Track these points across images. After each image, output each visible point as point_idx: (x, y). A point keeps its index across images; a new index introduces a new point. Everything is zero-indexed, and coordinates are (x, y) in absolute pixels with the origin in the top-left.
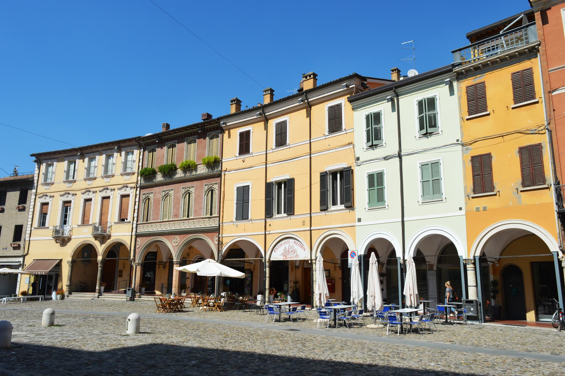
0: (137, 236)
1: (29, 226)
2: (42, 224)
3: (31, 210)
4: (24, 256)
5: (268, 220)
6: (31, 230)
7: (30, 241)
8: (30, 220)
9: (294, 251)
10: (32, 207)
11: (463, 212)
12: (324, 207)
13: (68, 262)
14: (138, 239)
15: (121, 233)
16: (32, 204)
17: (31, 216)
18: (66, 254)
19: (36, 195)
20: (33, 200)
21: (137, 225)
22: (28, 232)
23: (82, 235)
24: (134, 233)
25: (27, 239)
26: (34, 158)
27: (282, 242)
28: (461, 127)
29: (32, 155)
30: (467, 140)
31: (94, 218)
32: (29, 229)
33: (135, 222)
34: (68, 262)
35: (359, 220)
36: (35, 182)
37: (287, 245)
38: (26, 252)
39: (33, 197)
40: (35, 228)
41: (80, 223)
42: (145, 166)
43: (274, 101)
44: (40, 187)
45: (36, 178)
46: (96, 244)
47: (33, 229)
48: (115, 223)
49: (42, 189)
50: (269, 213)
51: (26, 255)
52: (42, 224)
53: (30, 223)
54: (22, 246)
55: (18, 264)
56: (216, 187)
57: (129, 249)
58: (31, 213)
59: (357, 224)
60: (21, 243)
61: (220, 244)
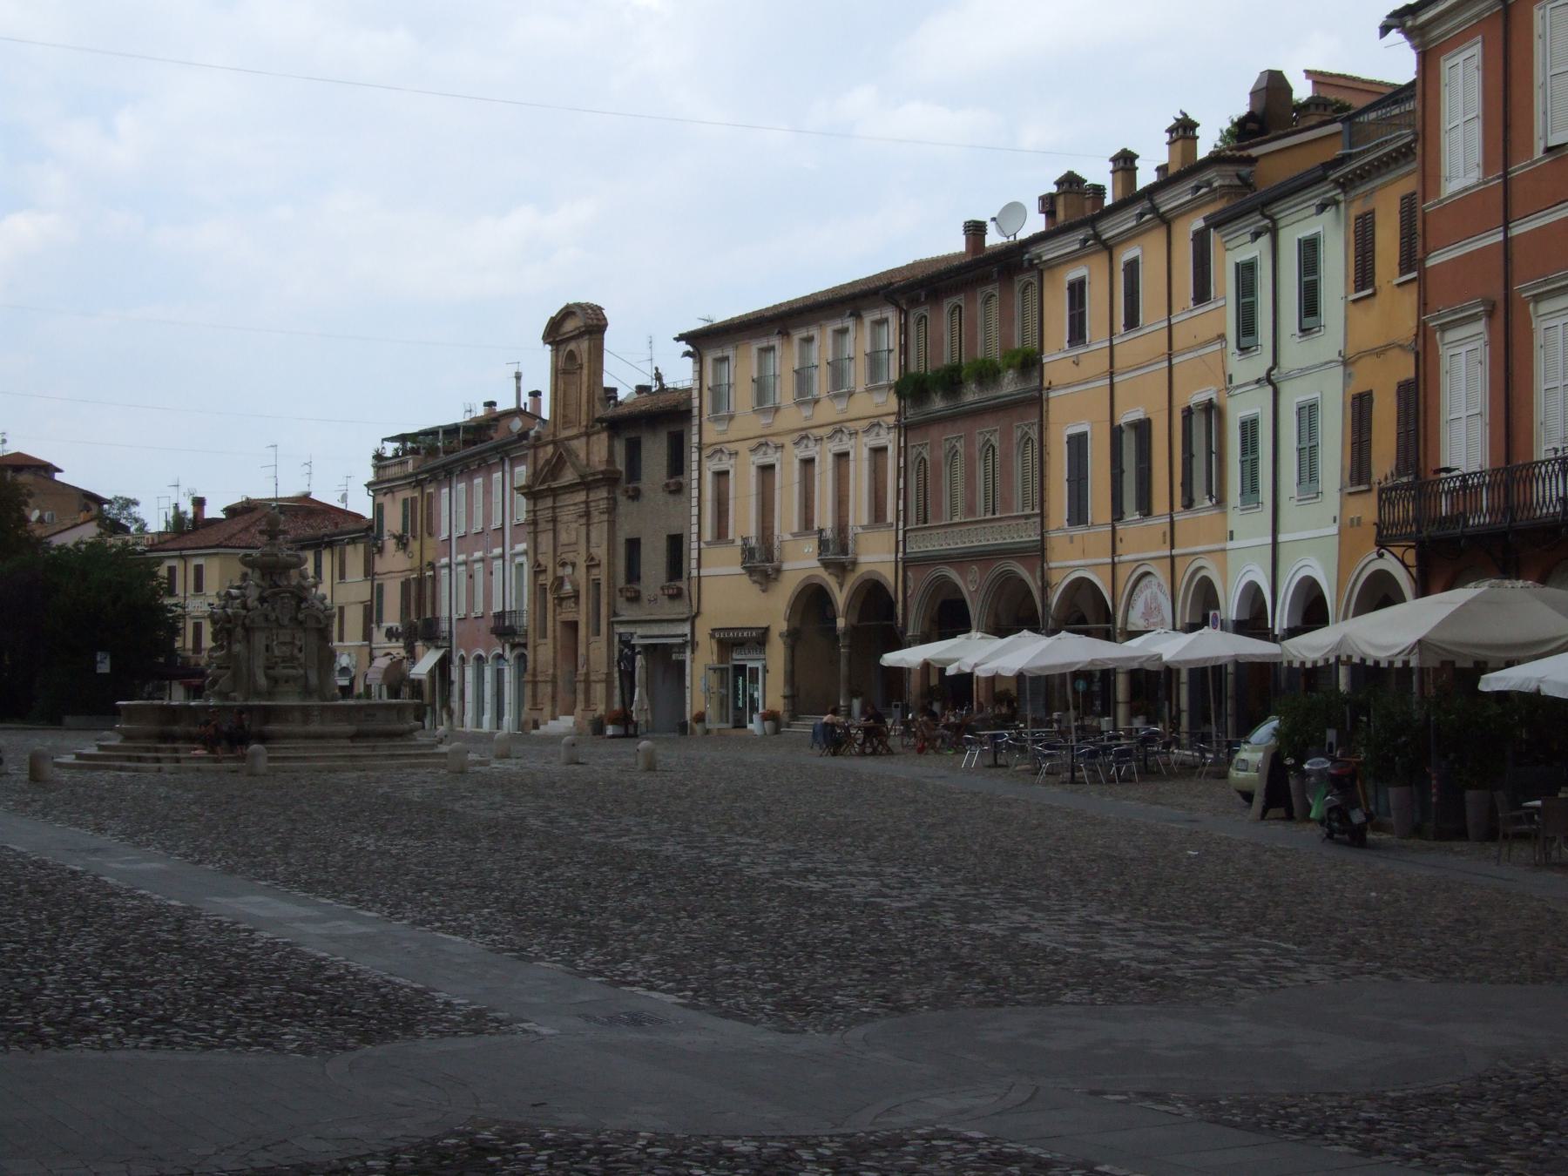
1: (694, 538)
2: (721, 533)
3: (695, 493)
4: (692, 619)
5: (1119, 527)
8: (694, 520)
10: (695, 484)
13: (781, 635)
15: (876, 556)
16: (695, 475)
17: (695, 511)
18: (771, 610)
19: (700, 449)
20: (695, 466)
21: (905, 533)
22: (694, 554)
23: (801, 562)
25: (694, 573)
26: (685, 346)
27: (1142, 584)
28: (1346, 318)
29: (677, 339)
30: (1350, 353)
32: (694, 545)
33: (901, 524)
34: (781, 635)
36: (695, 412)
38: (695, 609)
39: (695, 457)
40: (707, 543)
41: (796, 529)
42: (913, 369)
43: (1139, 187)
44: (707, 426)
45: (696, 403)
46: (831, 582)
48: (863, 527)
49: (712, 433)
51: (698, 613)
52: (721, 533)
53: (695, 529)
54: (686, 592)
55: (680, 640)
58: (694, 502)
59: (1230, 545)
60: (683, 585)
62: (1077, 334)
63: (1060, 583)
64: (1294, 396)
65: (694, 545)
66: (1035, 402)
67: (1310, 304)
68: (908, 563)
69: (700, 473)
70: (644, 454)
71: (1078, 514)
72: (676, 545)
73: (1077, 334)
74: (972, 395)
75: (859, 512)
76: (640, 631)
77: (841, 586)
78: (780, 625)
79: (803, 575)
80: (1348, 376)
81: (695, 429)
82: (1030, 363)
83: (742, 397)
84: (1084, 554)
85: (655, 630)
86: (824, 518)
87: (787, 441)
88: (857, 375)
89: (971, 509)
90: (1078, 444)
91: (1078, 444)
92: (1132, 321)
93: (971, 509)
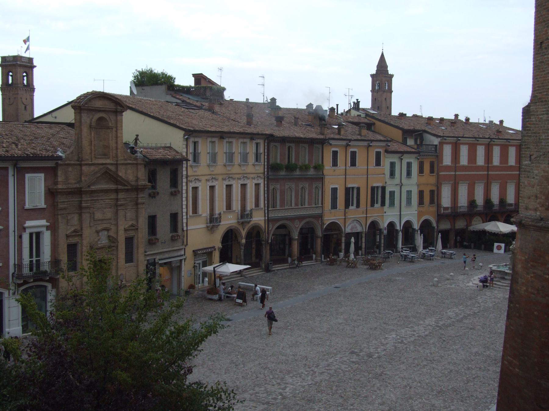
0: (269, 220)
1: (184, 214)
6: (187, 218)
7: (187, 230)
8: (184, 207)
9: (356, 227)
11: (416, 212)
12: (372, 205)
14: (270, 223)
19: (187, 178)
23: (229, 221)
24: (266, 218)
25: (185, 229)
31: (236, 205)
32: (185, 217)
35: (385, 212)
37: (353, 224)
39: (184, 180)
47: (188, 217)
50: (347, 206)
53: (184, 210)
56: (320, 185)
57: (264, 231)
61: (323, 224)
62: (335, 164)
63: (327, 223)
64: (404, 190)
65: (185, 217)
66: (321, 179)
67: (409, 174)
68: (269, 221)
69: (186, 188)
70: (158, 177)
71: (334, 206)
72: (174, 218)
73: (335, 164)
74: (298, 172)
75: (250, 205)
76: (158, 257)
77: (244, 229)
78: (219, 245)
79: (229, 226)
80: (418, 187)
81: (184, 169)
82: (319, 168)
83: (204, 159)
84: (335, 216)
85: (167, 256)
86: (236, 205)
87: (220, 178)
88: (251, 159)
89: (291, 205)
90: (334, 191)
91: (334, 191)
92: (353, 164)
93: (296, 204)
